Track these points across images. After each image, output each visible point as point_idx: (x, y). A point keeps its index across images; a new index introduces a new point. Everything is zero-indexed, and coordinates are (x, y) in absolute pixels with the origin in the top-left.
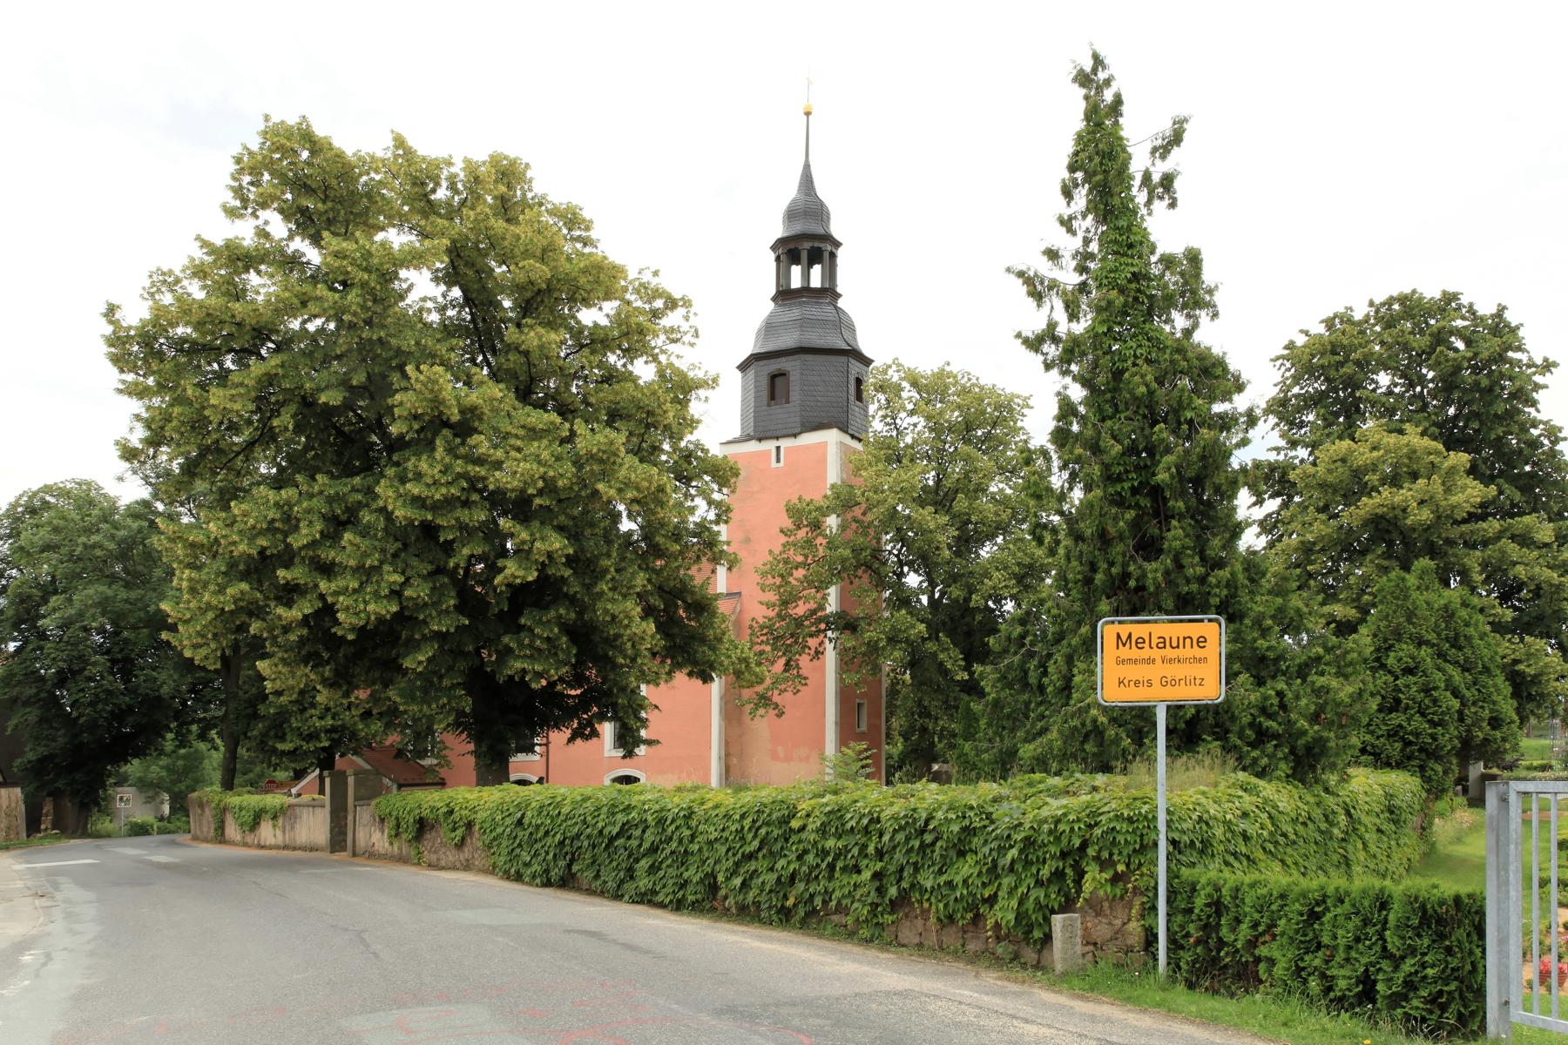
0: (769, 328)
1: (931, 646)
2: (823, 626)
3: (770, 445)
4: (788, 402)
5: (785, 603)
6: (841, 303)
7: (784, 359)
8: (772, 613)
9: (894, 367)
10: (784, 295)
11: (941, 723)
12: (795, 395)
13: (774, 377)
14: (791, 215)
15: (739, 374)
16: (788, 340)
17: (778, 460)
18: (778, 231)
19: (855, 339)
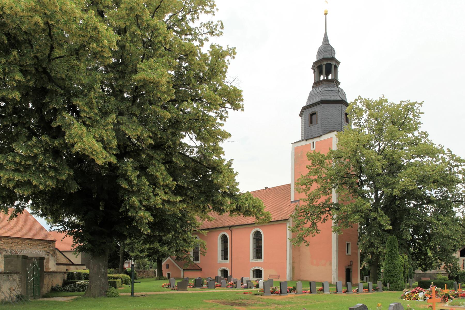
0: (311, 96)
1: (373, 215)
3: (310, 142)
4: (317, 124)
7: (315, 107)
10: (317, 84)
11: (379, 250)
12: (319, 121)
13: (312, 115)
15: (300, 118)
16: (317, 99)
17: (313, 147)
18: (315, 59)
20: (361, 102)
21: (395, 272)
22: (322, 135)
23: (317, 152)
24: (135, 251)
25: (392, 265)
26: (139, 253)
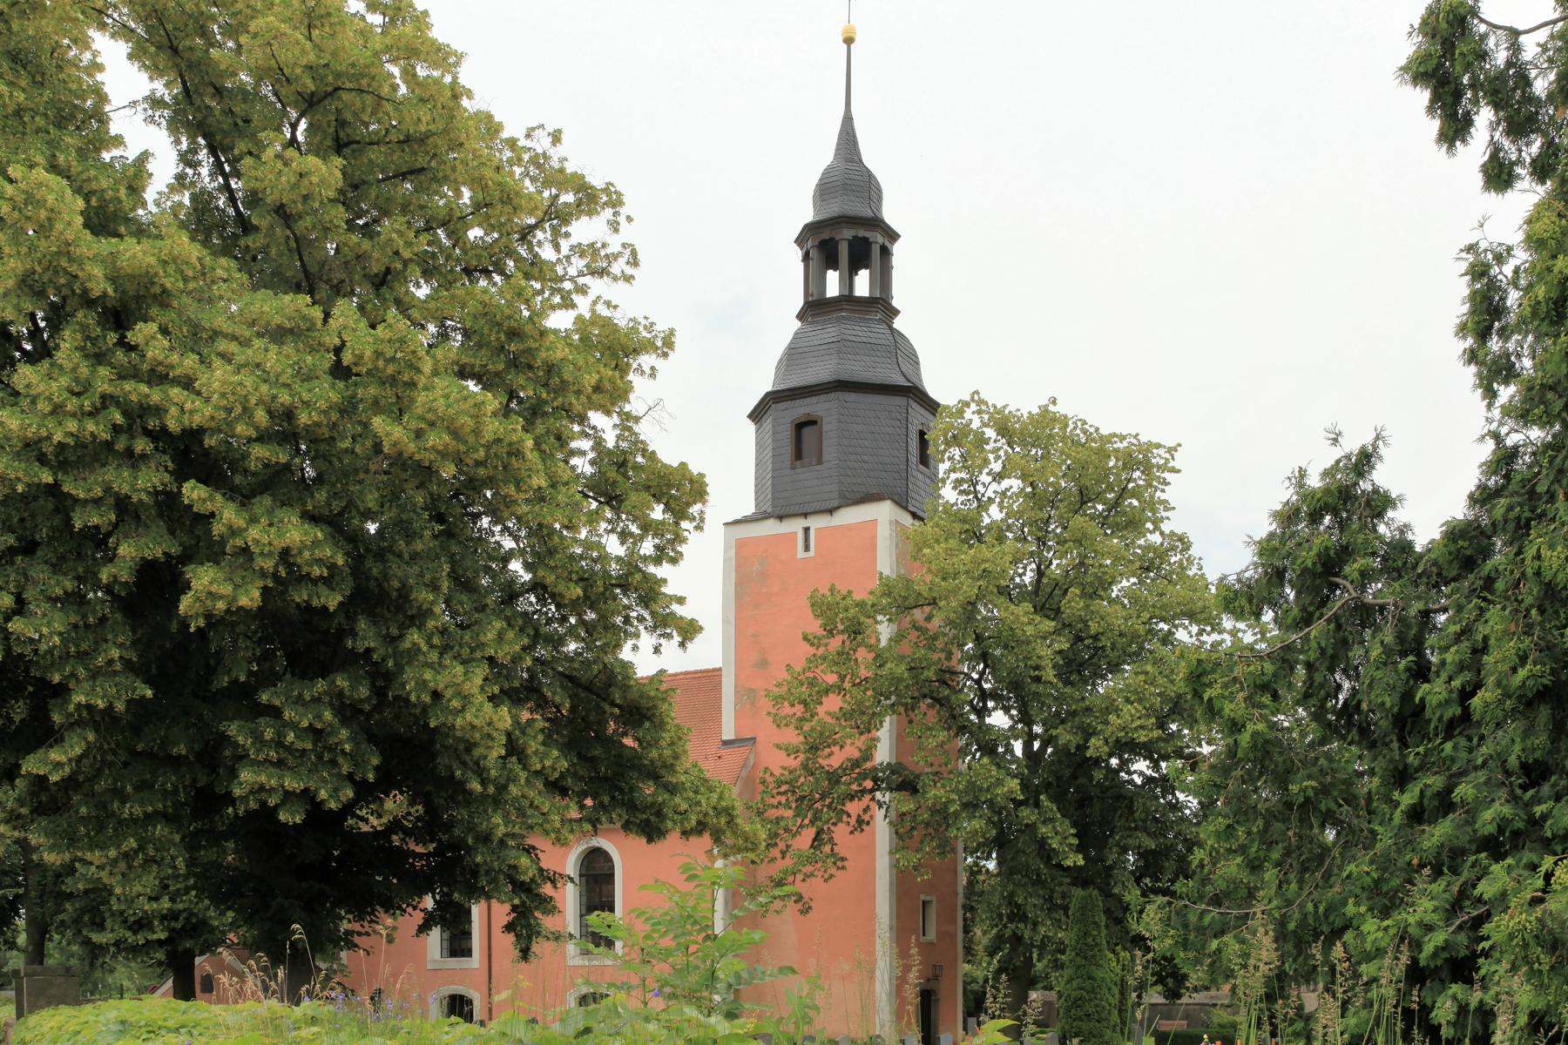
0: (793, 355)
2: (869, 784)
4: (820, 462)
5: (814, 749)
6: (898, 324)
7: (814, 399)
8: (793, 763)
9: (973, 407)
10: (815, 308)
12: (830, 452)
13: (800, 426)
14: (826, 189)
18: (806, 213)
19: (921, 380)
20: (979, 412)
21: (1097, 1006)
22: (839, 508)
23: (844, 592)
24: (108, 924)
25: (1088, 984)
26: (128, 934)
